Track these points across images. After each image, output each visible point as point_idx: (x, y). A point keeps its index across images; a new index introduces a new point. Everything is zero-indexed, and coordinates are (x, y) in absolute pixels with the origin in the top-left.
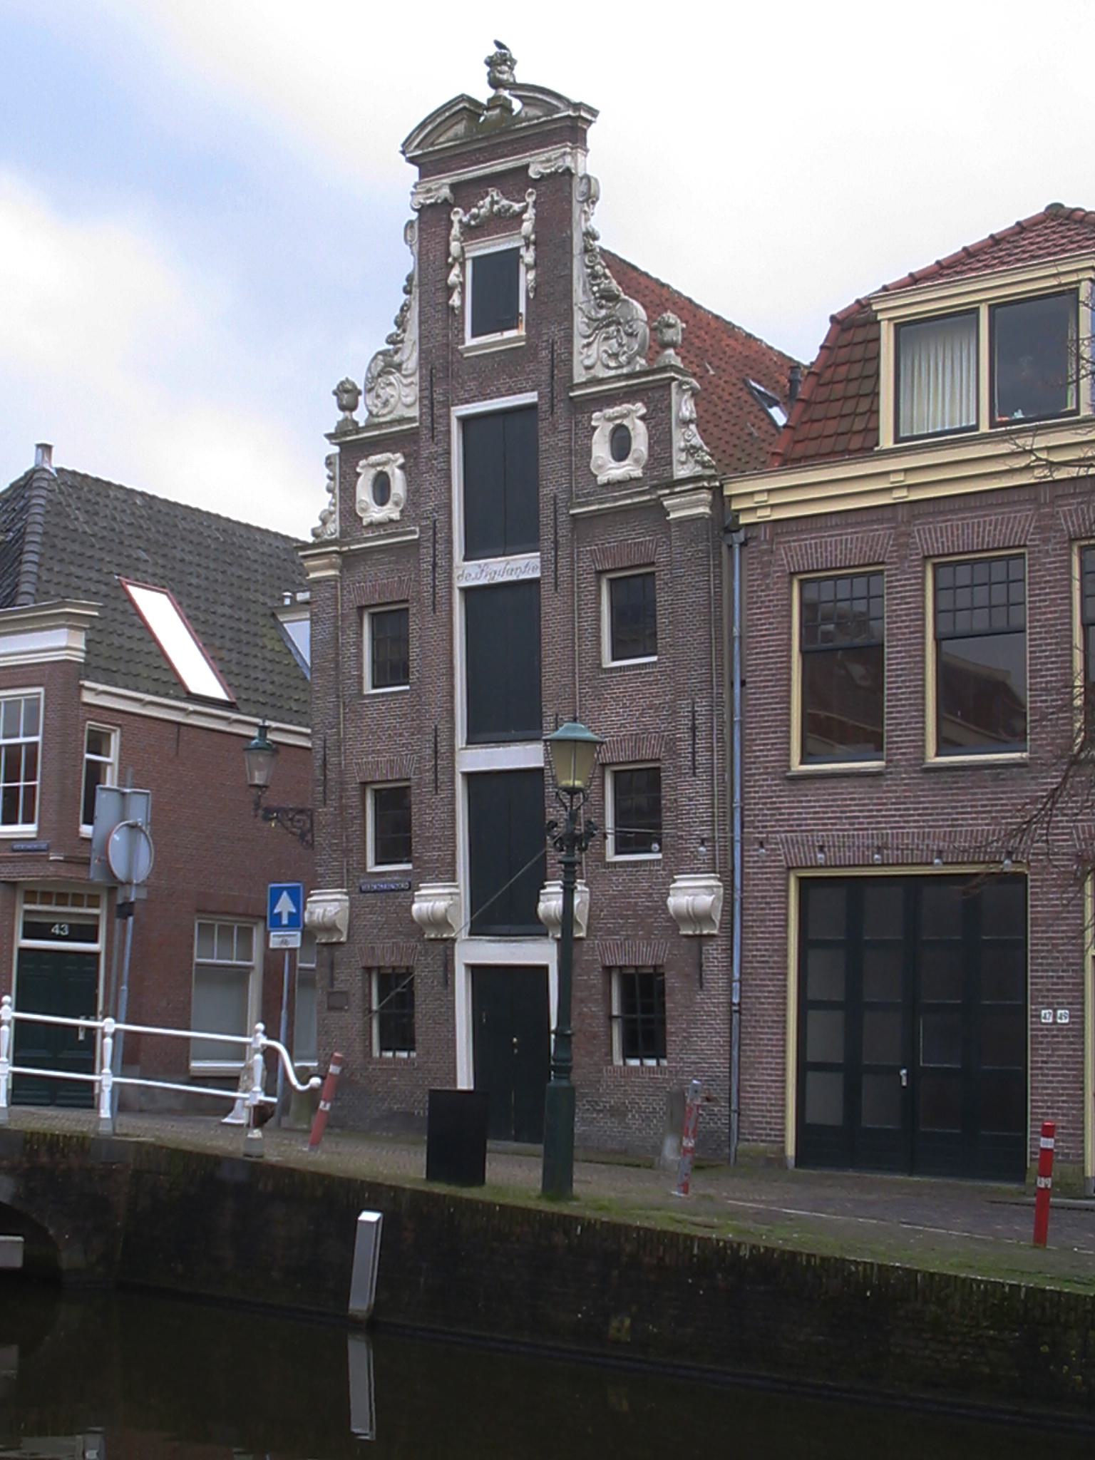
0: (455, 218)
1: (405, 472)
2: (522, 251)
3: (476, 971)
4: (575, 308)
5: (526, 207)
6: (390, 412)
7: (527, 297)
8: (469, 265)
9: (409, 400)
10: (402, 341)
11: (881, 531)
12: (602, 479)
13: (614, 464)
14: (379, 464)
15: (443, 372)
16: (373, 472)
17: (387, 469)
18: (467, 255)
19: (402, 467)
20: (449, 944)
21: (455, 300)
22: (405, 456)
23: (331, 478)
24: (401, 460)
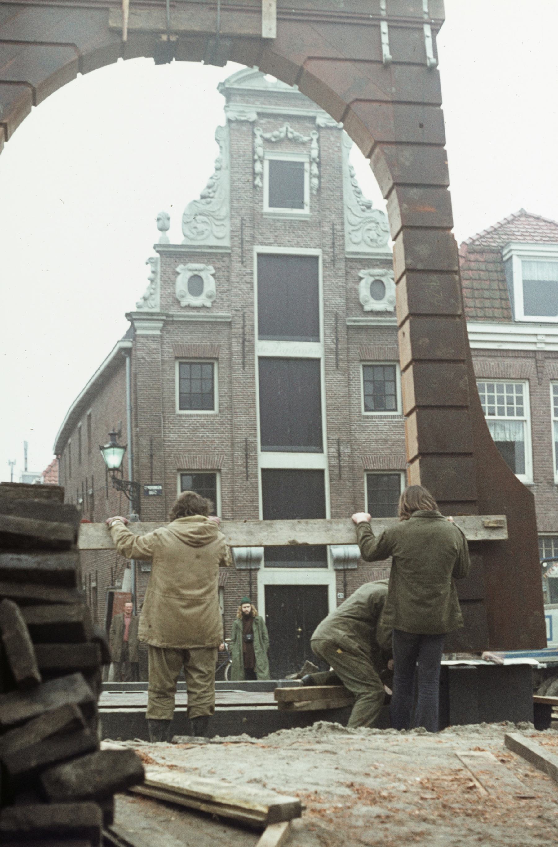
0: (258, 133)
1: (215, 278)
2: (307, 166)
3: (269, 589)
4: (345, 207)
5: (312, 140)
6: (203, 240)
7: (311, 194)
8: (267, 164)
9: (220, 235)
10: (212, 198)
11: (530, 363)
12: (367, 308)
13: (372, 301)
14: (196, 270)
15: (249, 224)
16: (190, 274)
17: (202, 274)
18: (266, 157)
19: (213, 275)
20: (252, 573)
21: (258, 181)
22: (215, 269)
23: (153, 272)
24: (213, 271)
